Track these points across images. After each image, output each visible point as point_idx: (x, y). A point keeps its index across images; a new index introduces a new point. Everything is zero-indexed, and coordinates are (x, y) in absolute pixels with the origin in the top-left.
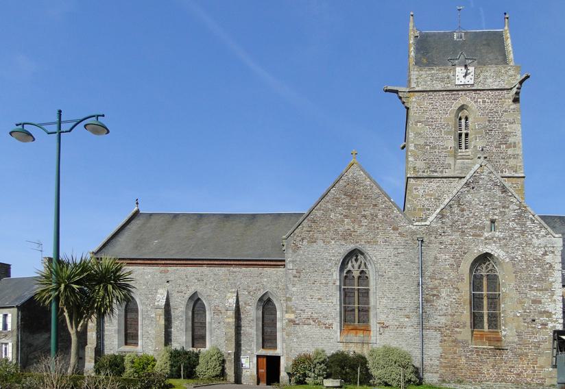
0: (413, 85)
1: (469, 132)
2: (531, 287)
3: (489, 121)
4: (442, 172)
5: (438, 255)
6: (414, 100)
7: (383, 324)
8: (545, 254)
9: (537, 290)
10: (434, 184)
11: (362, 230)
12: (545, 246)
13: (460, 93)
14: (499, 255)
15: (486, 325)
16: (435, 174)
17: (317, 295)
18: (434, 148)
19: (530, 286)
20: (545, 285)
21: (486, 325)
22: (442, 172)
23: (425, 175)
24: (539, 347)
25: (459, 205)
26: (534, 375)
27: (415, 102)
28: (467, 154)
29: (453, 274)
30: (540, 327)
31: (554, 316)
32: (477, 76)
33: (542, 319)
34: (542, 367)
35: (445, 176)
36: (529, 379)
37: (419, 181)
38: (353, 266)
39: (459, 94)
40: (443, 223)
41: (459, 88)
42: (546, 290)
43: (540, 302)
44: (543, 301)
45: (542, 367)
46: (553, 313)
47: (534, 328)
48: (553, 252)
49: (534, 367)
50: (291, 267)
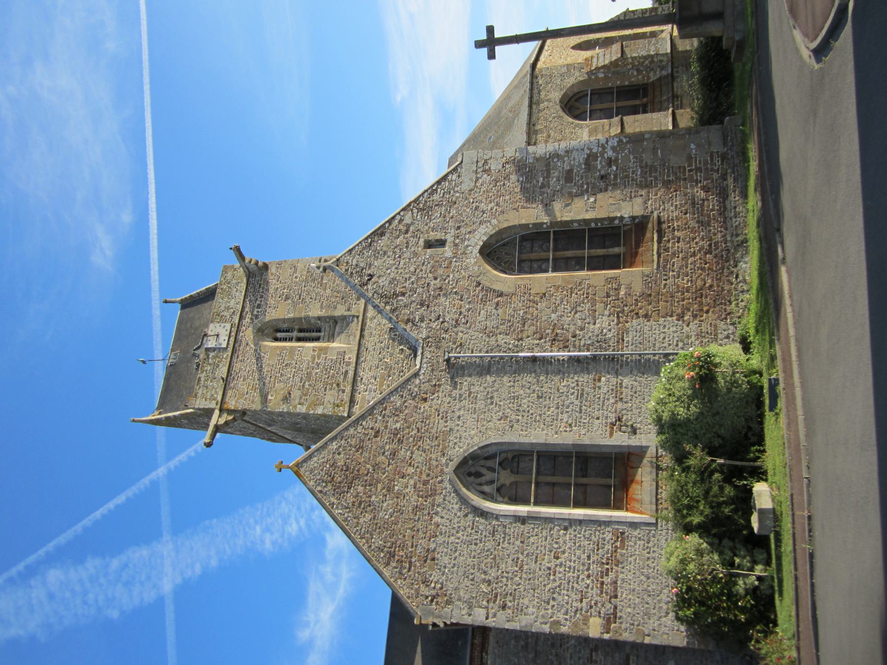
0: (212, 405)
1: (296, 327)
2: (543, 186)
3: (287, 298)
4: (348, 364)
5: (479, 326)
6: (233, 403)
7: (613, 424)
8: (487, 171)
9: (548, 176)
10: (365, 374)
11: (419, 457)
12: (476, 172)
13: (239, 338)
14: (485, 234)
15: (616, 250)
16: (351, 374)
17: (547, 561)
18: (309, 375)
19: (541, 188)
20: (540, 166)
21: (616, 250)
22: (348, 364)
23: (348, 389)
24: (651, 166)
25: (396, 295)
26: (707, 169)
27: (236, 402)
28: (327, 329)
29: (516, 303)
30: (614, 168)
31: (595, 151)
32: (223, 319)
33: (599, 167)
34: (689, 158)
35: (355, 360)
36: (715, 176)
37: (358, 397)
38: (492, 482)
39: (241, 341)
40: (422, 320)
41: (232, 339)
42: (548, 165)
43: (570, 172)
44: (568, 168)
45: (689, 158)
46: (588, 152)
47: (616, 176)
48: (486, 162)
49: (690, 171)
50: (483, 612)
